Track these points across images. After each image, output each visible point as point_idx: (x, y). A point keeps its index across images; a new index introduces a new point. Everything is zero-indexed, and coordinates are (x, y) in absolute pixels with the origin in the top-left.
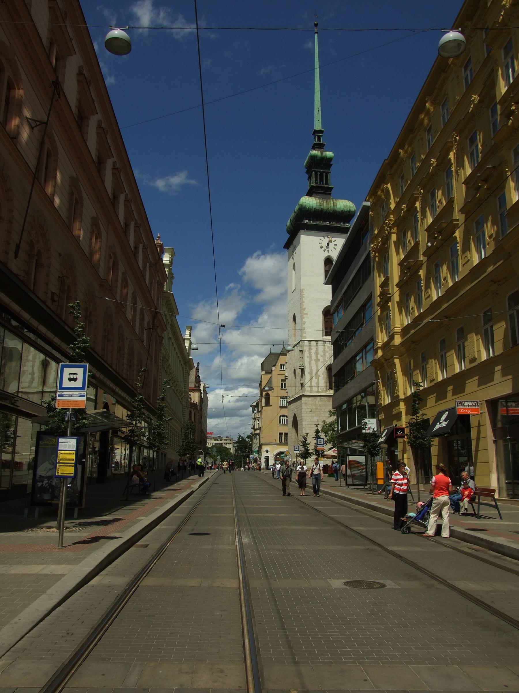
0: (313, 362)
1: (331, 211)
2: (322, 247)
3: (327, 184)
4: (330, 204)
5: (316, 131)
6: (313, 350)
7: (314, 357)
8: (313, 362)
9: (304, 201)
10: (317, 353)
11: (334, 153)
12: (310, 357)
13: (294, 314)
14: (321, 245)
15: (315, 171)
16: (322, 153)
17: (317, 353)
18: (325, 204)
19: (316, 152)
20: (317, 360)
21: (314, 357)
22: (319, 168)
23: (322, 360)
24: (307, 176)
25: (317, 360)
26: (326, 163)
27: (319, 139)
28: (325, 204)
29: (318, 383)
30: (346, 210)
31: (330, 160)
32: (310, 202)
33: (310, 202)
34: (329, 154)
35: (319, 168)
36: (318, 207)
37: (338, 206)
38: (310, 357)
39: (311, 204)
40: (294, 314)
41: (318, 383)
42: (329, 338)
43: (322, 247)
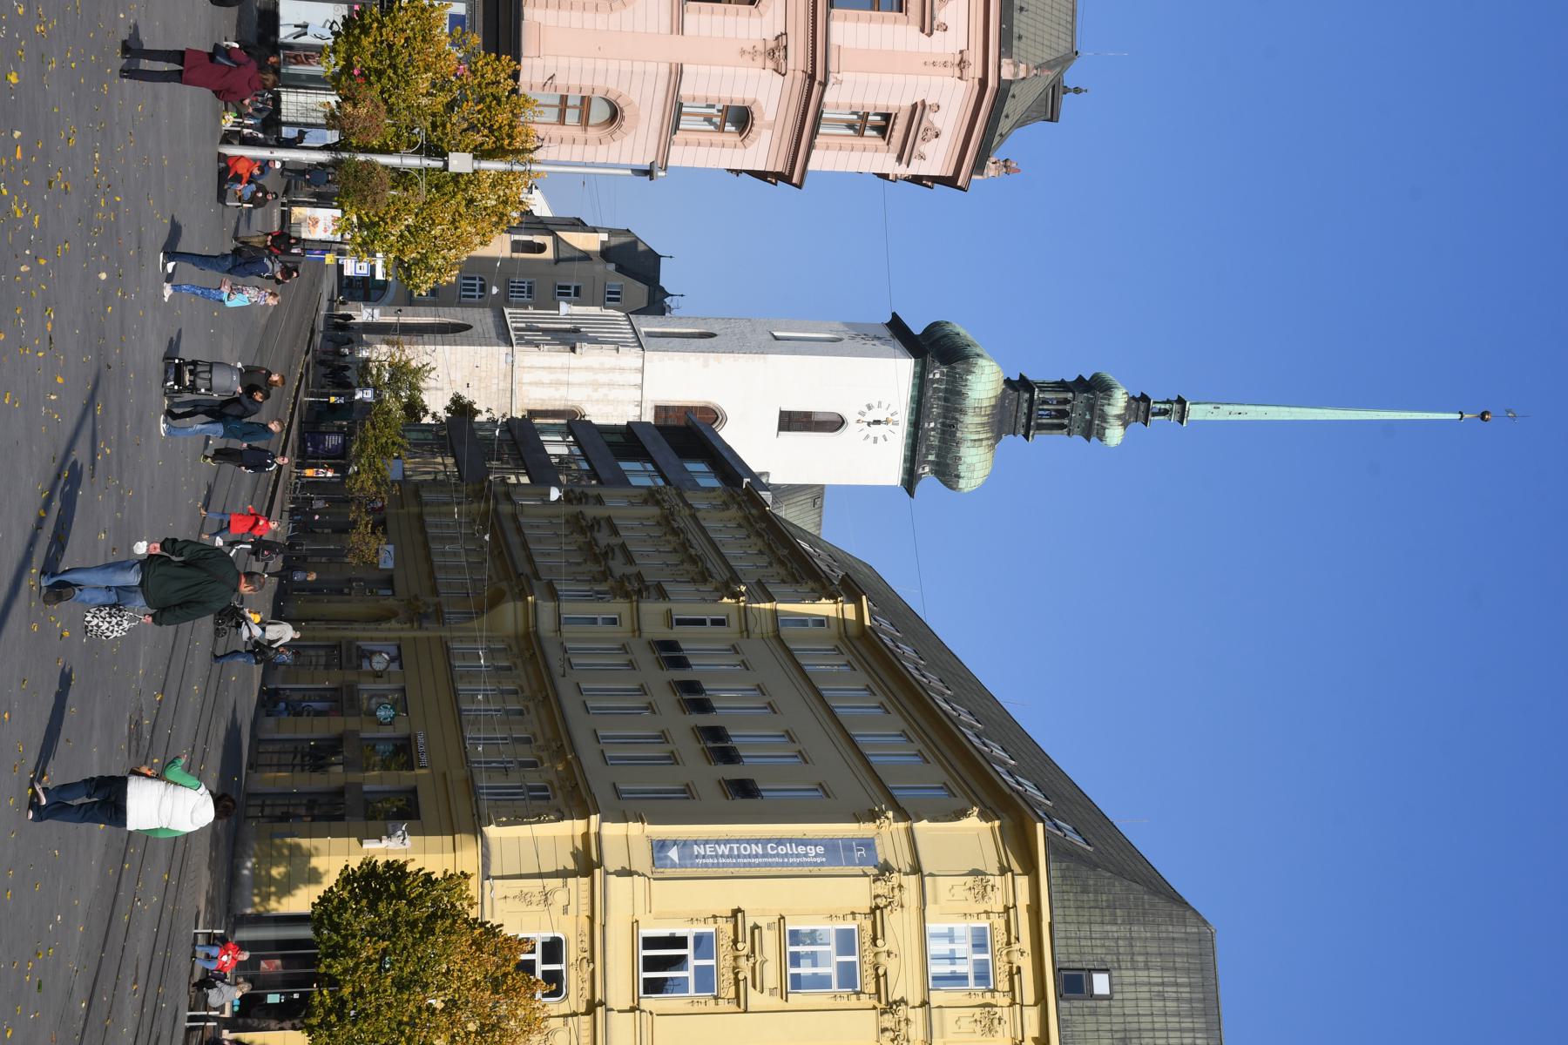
0: (589, 376)
1: (959, 434)
2: (869, 407)
3: (1040, 427)
5: (1181, 401)
6: (617, 377)
7: (603, 378)
8: (589, 376)
9: (987, 370)
10: (611, 385)
11: (1118, 447)
12: (603, 370)
14: (875, 404)
17: (611, 385)
18: (978, 420)
19: (1119, 402)
20: (596, 385)
21: (603, 378)
23: (595, 396)
24: (1071, 378)
25: (596, 385)
26: (1092, 429)
27: (1165, 412)
29: (539, 384)
30: (962, 469)
31: (1101, 437)
32: (984, 384)
33: (984, 384)
34: (1115, 434)
37: (973, 451)
38: (603, 370)
41: (539, 384)
42: (649, 417)
43: (869, 407)
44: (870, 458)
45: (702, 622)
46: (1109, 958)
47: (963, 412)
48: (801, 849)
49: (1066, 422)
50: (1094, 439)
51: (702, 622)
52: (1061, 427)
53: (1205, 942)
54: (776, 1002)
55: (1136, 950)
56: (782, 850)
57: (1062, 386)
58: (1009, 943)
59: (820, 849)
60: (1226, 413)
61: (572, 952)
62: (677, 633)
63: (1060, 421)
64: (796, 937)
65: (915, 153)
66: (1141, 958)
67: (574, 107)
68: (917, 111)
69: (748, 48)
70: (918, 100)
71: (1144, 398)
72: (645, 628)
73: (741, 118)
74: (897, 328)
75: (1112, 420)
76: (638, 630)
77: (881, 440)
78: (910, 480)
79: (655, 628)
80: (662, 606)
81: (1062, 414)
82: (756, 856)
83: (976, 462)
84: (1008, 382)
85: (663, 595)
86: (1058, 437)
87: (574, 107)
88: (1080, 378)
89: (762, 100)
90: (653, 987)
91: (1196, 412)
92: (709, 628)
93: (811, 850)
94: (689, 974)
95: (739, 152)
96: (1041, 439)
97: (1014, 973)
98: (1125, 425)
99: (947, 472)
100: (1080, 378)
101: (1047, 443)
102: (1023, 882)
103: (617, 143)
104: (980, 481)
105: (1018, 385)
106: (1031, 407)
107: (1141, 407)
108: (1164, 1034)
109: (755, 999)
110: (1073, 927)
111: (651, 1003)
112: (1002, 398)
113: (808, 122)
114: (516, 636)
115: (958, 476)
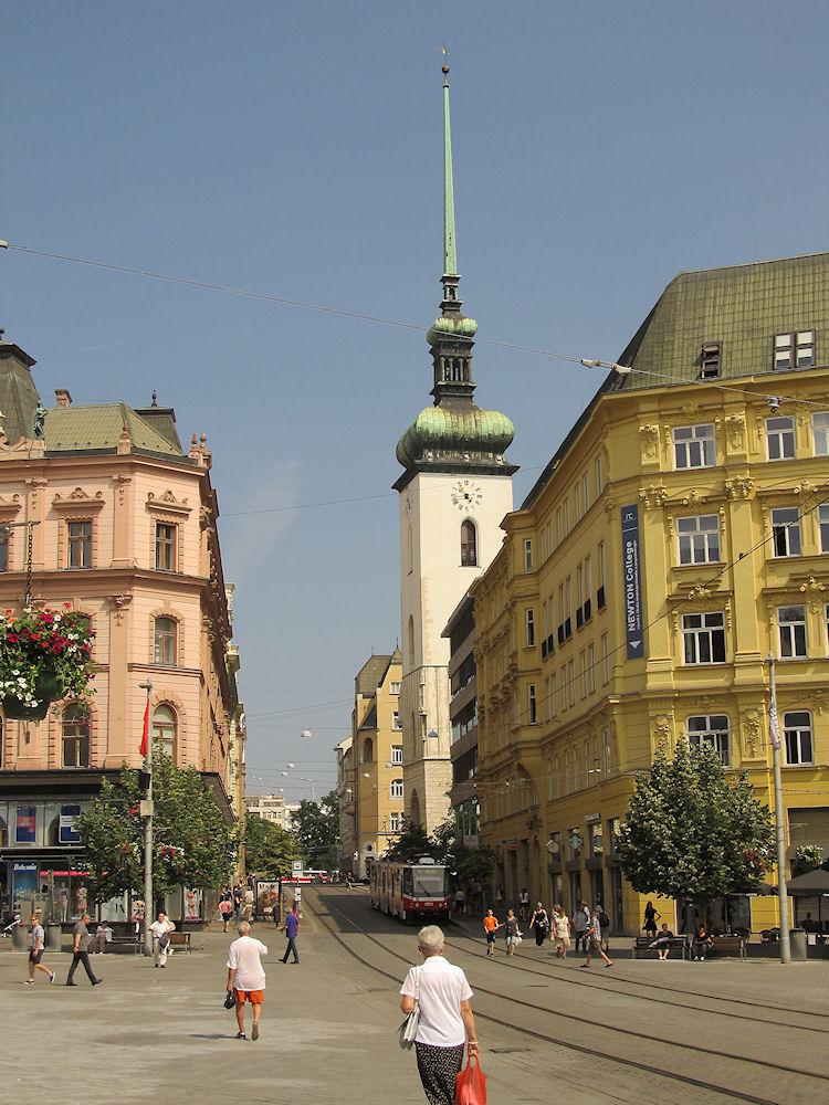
3: (467, 379)
4: (470, 423)
5: (444, 279)
9: (425, 420)
13: (411, 616)
15: (444, 356)
16: (456, 324)
19: (445, 323)
22: (450, 352)
24: (432, 359)
26: (464, 342)
27: (452, 292)
28: (461, 425)
31: (471, 334)
33: (436, 420)
34: (468, 324)
35: (450, 352)
36: (450, 431)
39: (437, 424)
40: (411, 616)
44: (495, 499)
45: (531, 626)
46: (696, 345)
47: (455, 436)
48: (629, 557)
49: (462, 360)
50: (473, 339)
51: (531, 626)
52: (466, 364)
53: (684, 279)
54: (726, 574)
55: (691, 326)
56: (630, 571)
57: (436, 365)
58: (683, 414)
59: (629, 544)
60: (451, 249)
61: (697, 712)
62: (538, 643)
63: (462, 365)
64: (685, 557)
65: (183, 506)
66: (697, 322)
67: (161, 733)
68: (151, 507)
69: (114, 621)
70: (144, 507)
71: (443, 305)
72: (536, 666)
73: (166, 622)
74: (401, 485)
75: (459, 328)
76: (538, 671)
77: (478, 493)
78: (508, 471)
79: (535, 659)
80: (521, 655)
81: (456, 364)
82: (634, 587)
83: (492, 422)
84: (436, 404)
85: (514, 655)
86: (473, 364)
87: (161, 733)
88: (431, 352)
89: (150, 610)
90: (720, 655)
91: (451, 271)
92: (535, 621)
93: (630, 551)
94: (710, 630)
95: (187, 622)
96: (475, 379)
97: (702, 411)
98: (462, 318)
99: (500, 444)
100: (431, 352)
101: (478, 373)
102: (643, 408)
103: (185, 703)
104: (506, 420)
105: (439, 395)
106: (453, 390)
107: (450, 307)
108: (746, 304)
109: (724, 586)
110: (674, 371)
111: (729, 658)
112: (444, 407)
113: (165, 579)
114: (543, 755)
115: (503, 435)
